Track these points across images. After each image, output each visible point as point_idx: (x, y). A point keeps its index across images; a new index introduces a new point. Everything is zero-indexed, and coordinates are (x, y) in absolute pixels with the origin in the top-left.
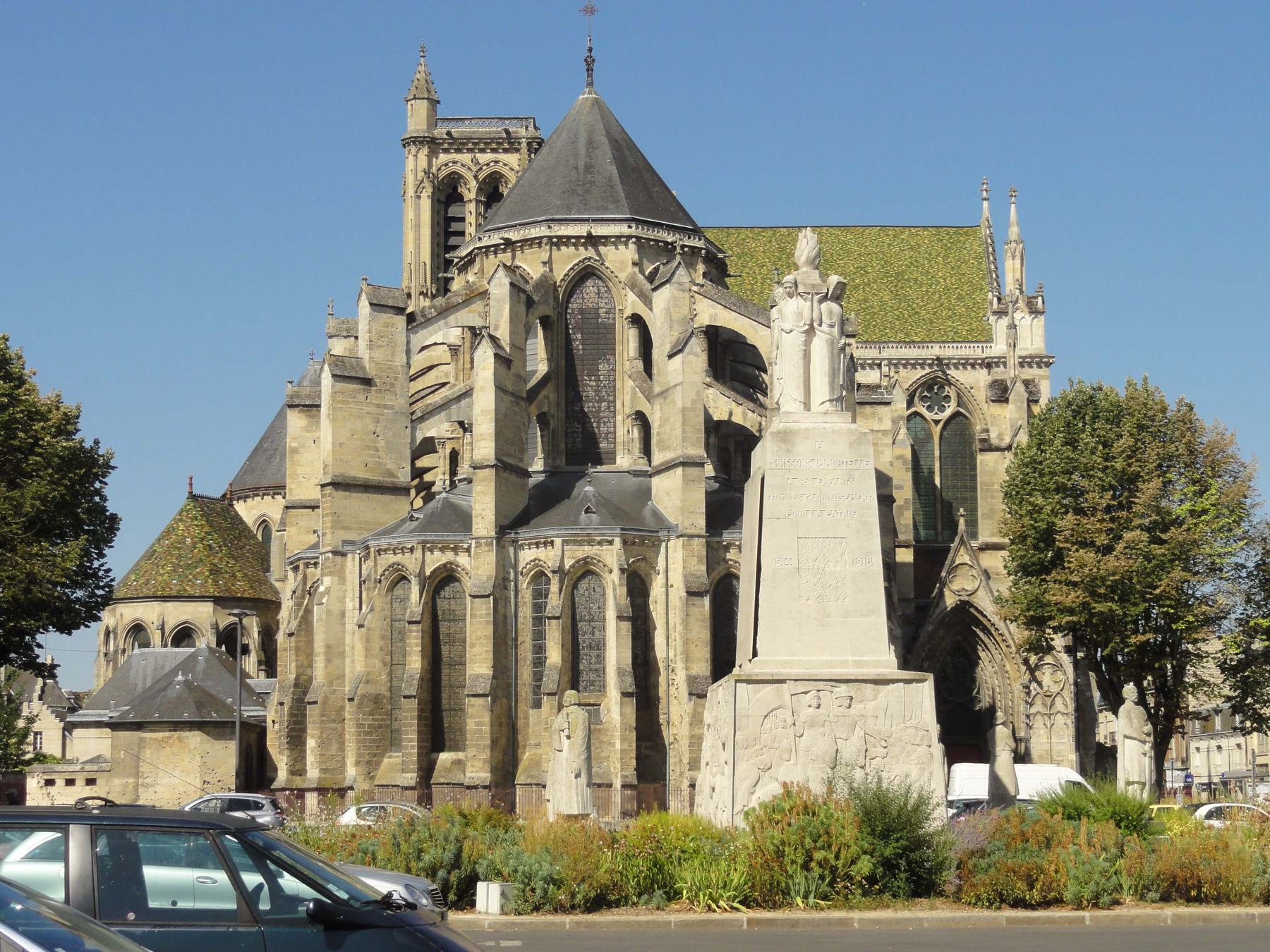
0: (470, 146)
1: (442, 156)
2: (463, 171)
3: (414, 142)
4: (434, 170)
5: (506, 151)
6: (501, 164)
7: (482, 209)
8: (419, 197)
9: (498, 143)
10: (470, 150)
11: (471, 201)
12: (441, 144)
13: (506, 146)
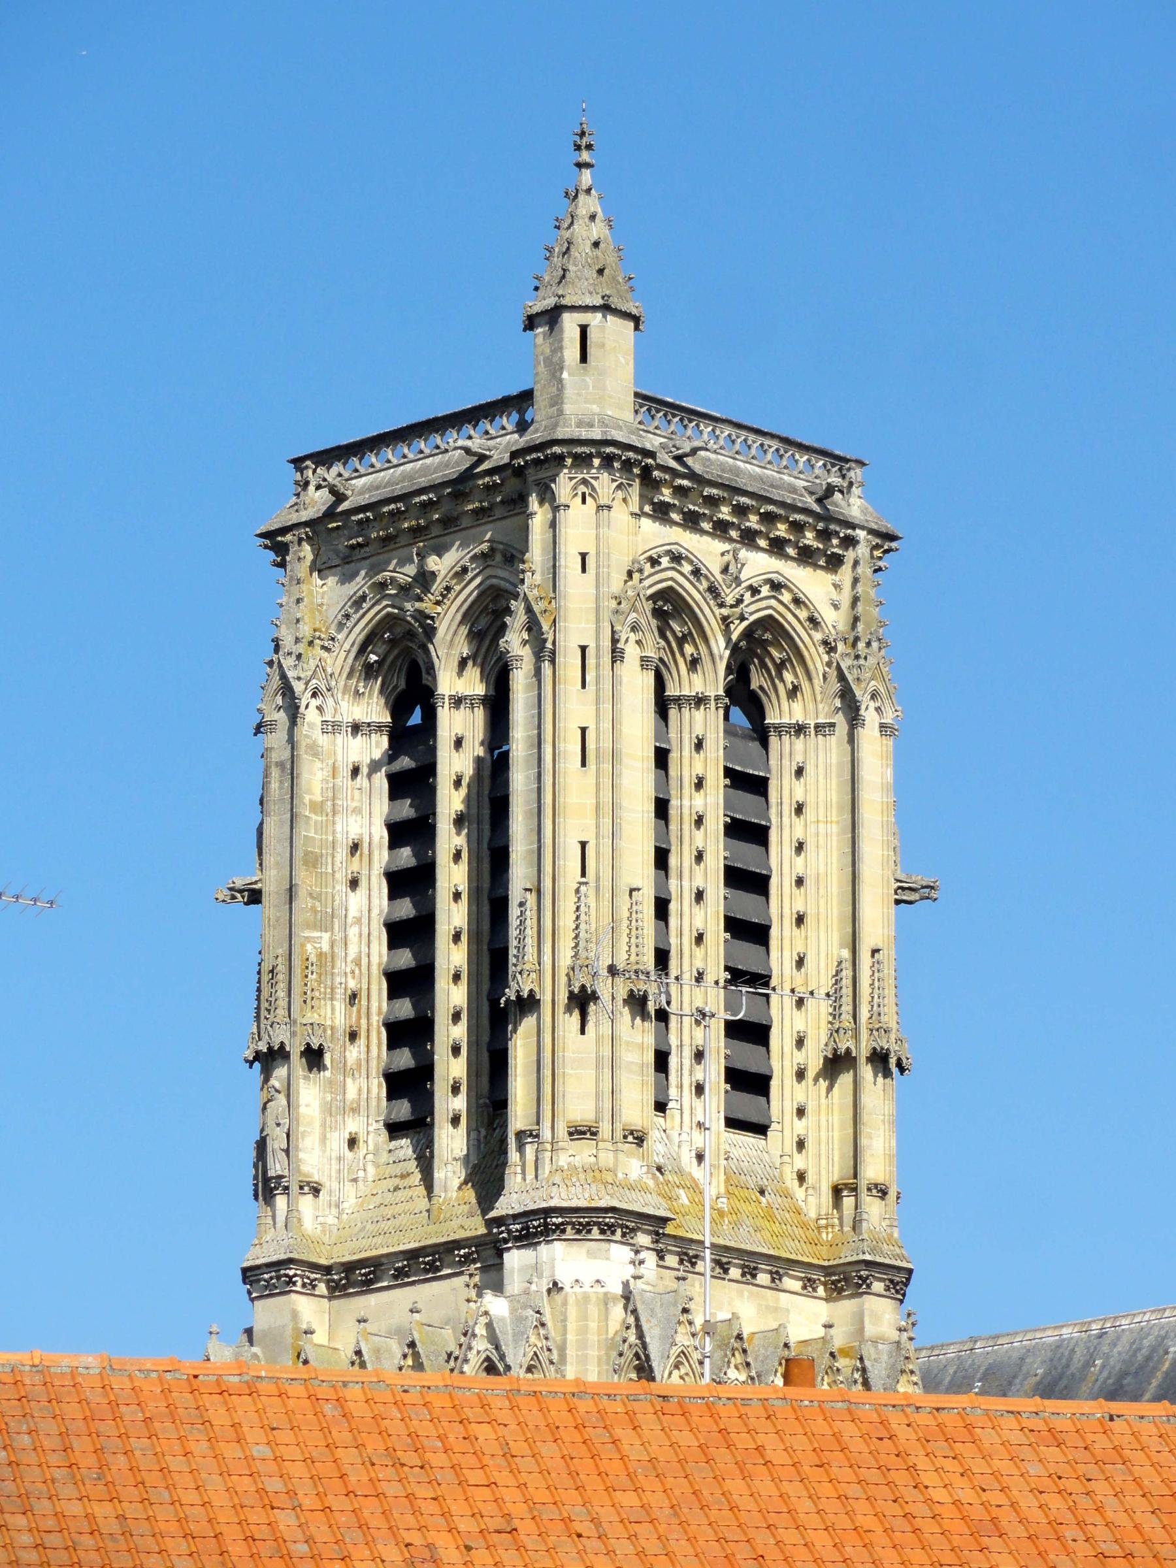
2: (694, 594)
5: (806, 556)
10: (721, 529)
11: (700, 701)
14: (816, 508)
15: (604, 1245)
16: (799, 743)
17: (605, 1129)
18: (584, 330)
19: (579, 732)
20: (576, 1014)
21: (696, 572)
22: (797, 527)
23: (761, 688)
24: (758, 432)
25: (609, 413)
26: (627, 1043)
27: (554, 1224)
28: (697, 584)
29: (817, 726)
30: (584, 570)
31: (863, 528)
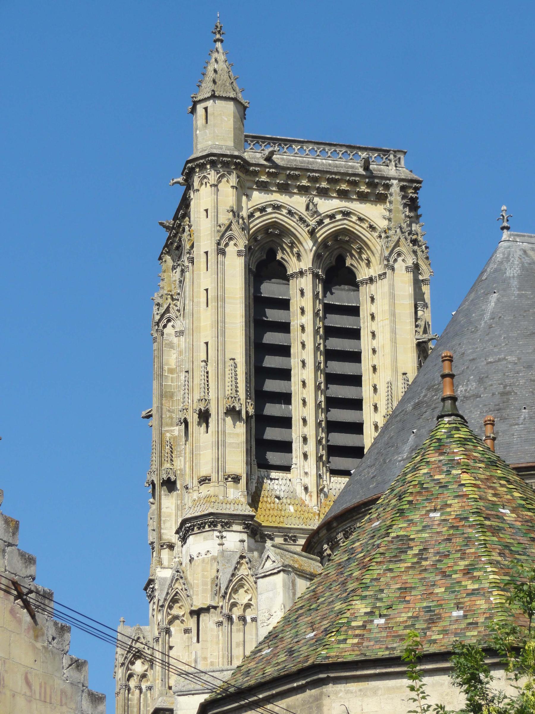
0: (304, 182)
1: (256, 194)
2: (291, 223)
3: (213, 164)
4: (244, 213)
5: (363, 197)
6: (354, 219)
7: (320, 288)
8: (222, 252)
9: (350, 183)
10: (304, 190)
11: (301, 273)
12: (256, 174)
13: (363, 188)
14: (361, 171)
15: (211, 533)
16: (373, 287)
17: (214, 478)
18: (206, 109)
19: (205, 292)
20: (204, 425)
21: (290, 212)
22: (354, 184)
23: (351, 265)
24: (330, 145)
25: (217, 143)
26: (230, 434)
27: (188, 527)
28: (292, 218)
29: (380, 276)
30: (207, 217)
31: (395, 179)
